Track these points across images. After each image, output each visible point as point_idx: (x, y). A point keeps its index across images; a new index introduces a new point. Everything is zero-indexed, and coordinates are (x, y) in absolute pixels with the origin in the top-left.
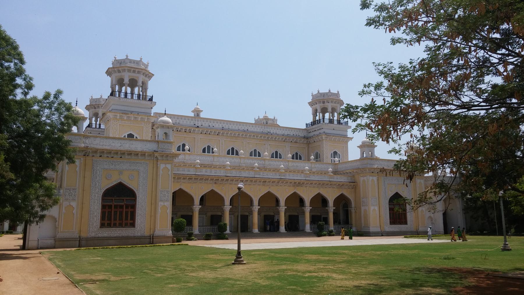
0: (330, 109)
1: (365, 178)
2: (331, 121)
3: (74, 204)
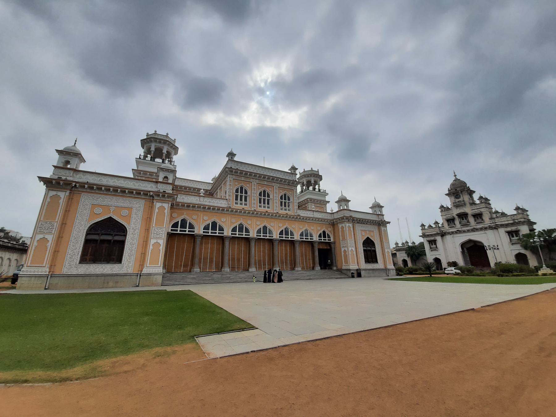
0: (313, 182)
1: (343, 225)
2: (314, 189)
3: (50, 237)
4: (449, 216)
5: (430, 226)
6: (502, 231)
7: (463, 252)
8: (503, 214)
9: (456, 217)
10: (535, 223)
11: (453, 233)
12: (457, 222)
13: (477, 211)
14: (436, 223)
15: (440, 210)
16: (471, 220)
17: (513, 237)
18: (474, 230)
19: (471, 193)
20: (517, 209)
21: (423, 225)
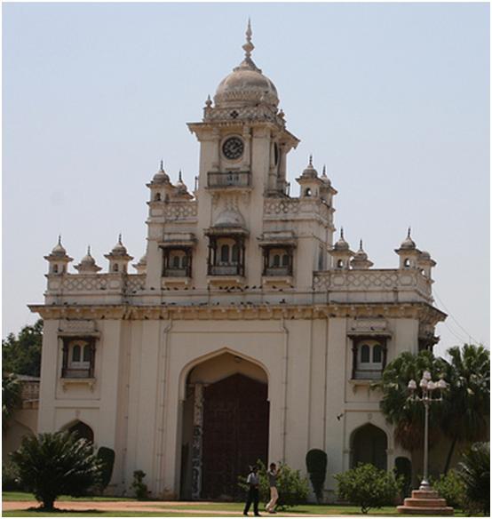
5: (89, 264)
6: (339, 328)
7: (187, 406)
8: (361, 259)
9: (205, 242)
10: (442, 316)
11: (167, 313)
12: (200, 263)
14: (119, 255)
15: (147, 195)
16: (254, 261)
17: (365, 359)
18: (257, 311)
19: (282, 143)
20: (408, 249)
21: (58, 257)
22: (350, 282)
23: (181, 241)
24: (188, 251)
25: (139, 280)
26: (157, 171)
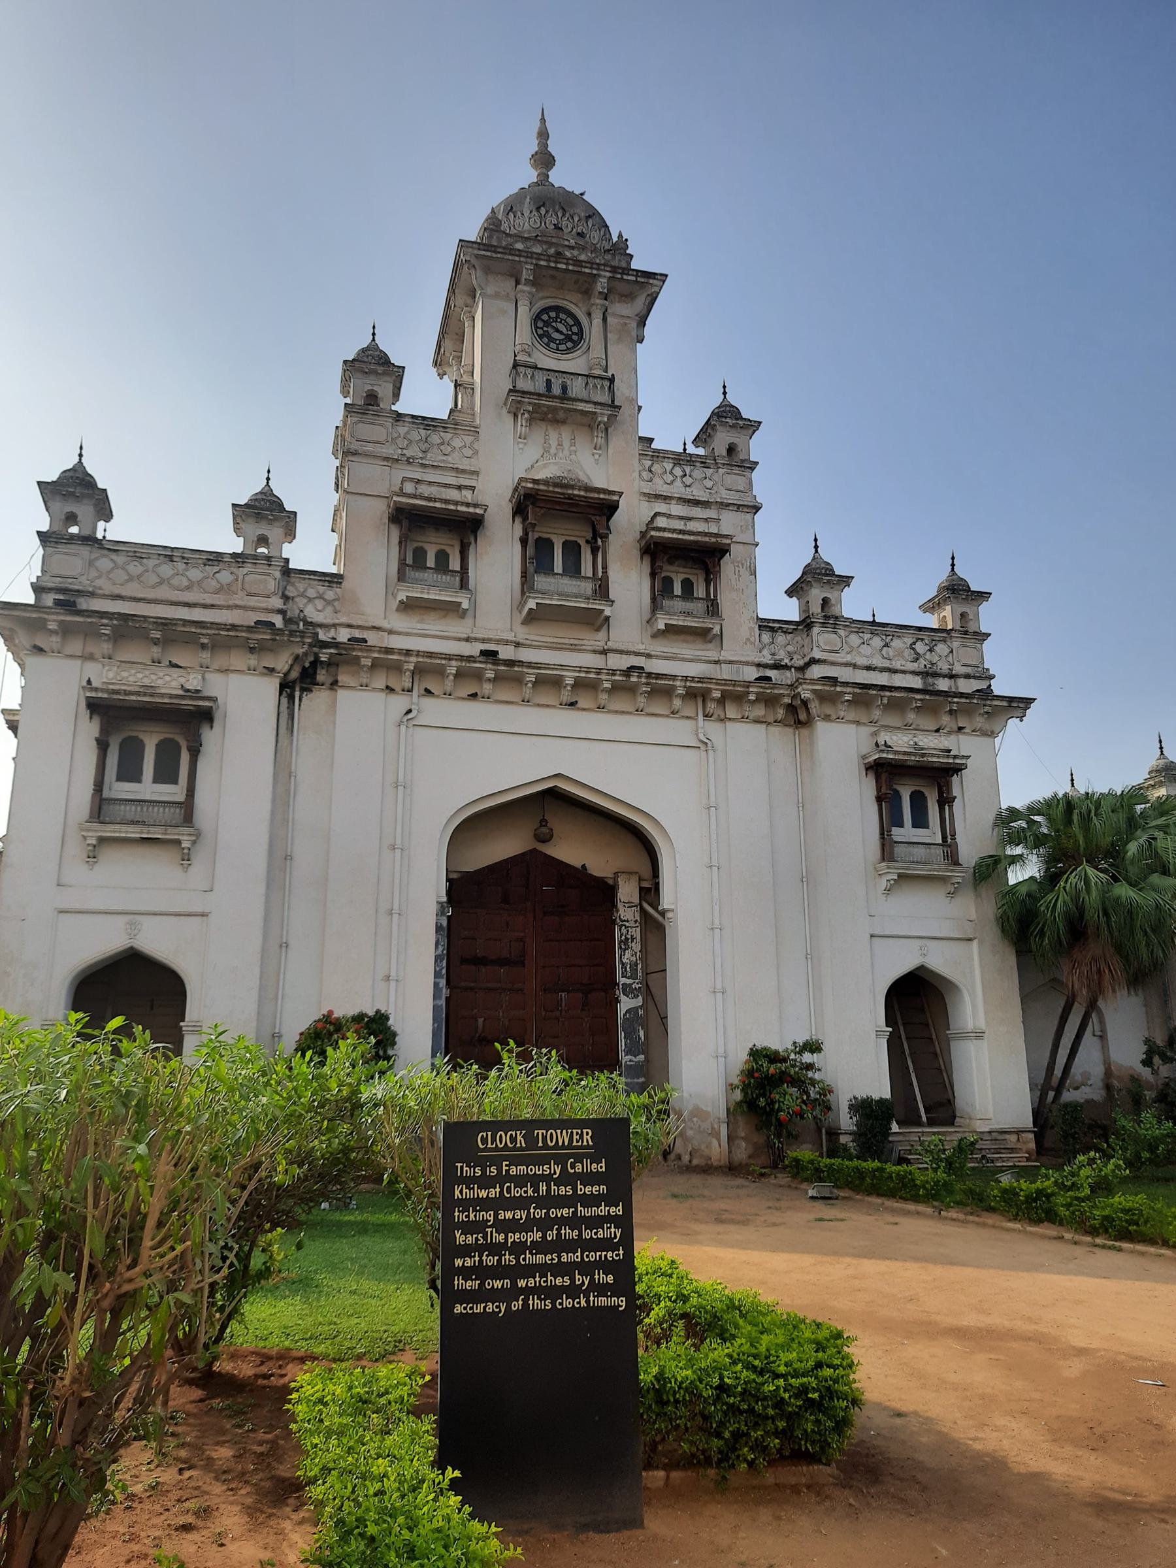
4: (438, 490)
6: (842, 744)
12: (497, 561)
13: (676, 522)
18: (639, 688)
22: (852, 649)
23: (447, 502)
24: (466, 527)
25: (321, 589)
26: (366, 342)
